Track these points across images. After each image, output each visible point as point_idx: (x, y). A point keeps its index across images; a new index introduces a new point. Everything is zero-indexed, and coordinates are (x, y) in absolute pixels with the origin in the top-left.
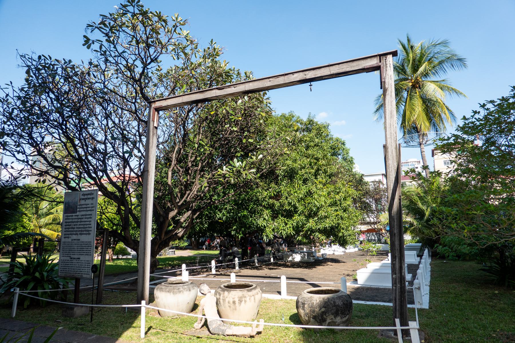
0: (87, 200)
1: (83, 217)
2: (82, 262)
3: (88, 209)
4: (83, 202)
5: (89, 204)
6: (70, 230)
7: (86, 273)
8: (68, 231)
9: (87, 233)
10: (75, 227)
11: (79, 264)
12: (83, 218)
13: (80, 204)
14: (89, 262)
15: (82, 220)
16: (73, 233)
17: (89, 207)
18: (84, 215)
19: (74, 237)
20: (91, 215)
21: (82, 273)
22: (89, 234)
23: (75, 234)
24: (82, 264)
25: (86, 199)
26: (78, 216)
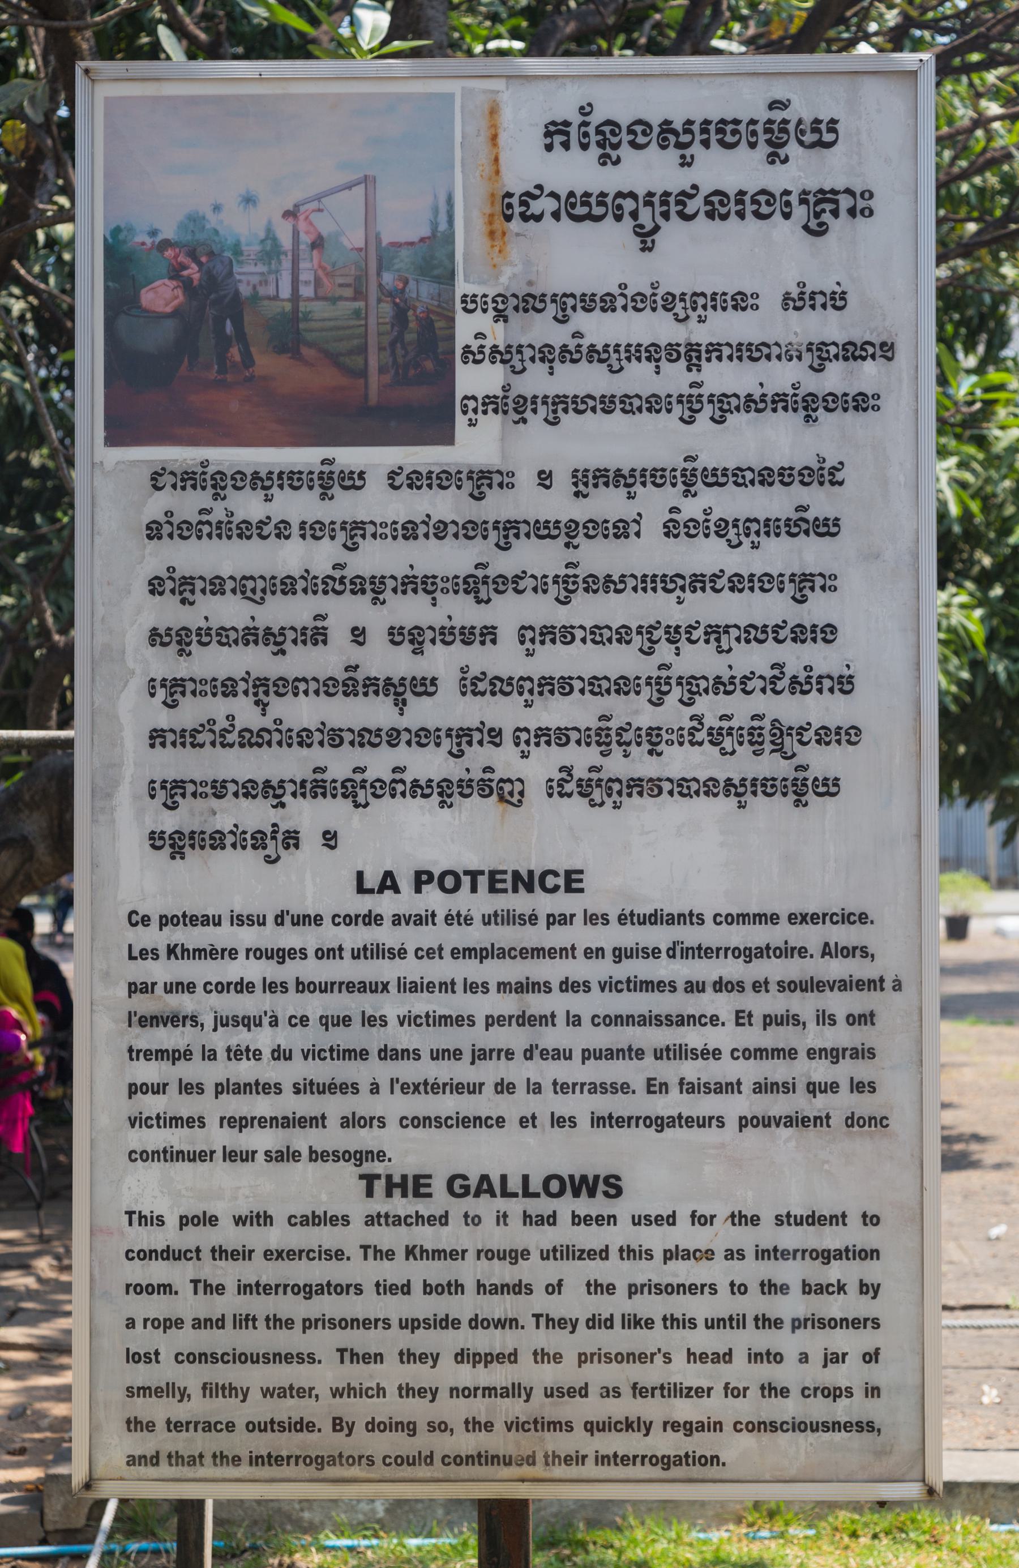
5: (741, 302)
7: (789, 1408)
12: (621, 530)
14: (854, 1235)
21: (684, 1410)
24: (682, 1272)
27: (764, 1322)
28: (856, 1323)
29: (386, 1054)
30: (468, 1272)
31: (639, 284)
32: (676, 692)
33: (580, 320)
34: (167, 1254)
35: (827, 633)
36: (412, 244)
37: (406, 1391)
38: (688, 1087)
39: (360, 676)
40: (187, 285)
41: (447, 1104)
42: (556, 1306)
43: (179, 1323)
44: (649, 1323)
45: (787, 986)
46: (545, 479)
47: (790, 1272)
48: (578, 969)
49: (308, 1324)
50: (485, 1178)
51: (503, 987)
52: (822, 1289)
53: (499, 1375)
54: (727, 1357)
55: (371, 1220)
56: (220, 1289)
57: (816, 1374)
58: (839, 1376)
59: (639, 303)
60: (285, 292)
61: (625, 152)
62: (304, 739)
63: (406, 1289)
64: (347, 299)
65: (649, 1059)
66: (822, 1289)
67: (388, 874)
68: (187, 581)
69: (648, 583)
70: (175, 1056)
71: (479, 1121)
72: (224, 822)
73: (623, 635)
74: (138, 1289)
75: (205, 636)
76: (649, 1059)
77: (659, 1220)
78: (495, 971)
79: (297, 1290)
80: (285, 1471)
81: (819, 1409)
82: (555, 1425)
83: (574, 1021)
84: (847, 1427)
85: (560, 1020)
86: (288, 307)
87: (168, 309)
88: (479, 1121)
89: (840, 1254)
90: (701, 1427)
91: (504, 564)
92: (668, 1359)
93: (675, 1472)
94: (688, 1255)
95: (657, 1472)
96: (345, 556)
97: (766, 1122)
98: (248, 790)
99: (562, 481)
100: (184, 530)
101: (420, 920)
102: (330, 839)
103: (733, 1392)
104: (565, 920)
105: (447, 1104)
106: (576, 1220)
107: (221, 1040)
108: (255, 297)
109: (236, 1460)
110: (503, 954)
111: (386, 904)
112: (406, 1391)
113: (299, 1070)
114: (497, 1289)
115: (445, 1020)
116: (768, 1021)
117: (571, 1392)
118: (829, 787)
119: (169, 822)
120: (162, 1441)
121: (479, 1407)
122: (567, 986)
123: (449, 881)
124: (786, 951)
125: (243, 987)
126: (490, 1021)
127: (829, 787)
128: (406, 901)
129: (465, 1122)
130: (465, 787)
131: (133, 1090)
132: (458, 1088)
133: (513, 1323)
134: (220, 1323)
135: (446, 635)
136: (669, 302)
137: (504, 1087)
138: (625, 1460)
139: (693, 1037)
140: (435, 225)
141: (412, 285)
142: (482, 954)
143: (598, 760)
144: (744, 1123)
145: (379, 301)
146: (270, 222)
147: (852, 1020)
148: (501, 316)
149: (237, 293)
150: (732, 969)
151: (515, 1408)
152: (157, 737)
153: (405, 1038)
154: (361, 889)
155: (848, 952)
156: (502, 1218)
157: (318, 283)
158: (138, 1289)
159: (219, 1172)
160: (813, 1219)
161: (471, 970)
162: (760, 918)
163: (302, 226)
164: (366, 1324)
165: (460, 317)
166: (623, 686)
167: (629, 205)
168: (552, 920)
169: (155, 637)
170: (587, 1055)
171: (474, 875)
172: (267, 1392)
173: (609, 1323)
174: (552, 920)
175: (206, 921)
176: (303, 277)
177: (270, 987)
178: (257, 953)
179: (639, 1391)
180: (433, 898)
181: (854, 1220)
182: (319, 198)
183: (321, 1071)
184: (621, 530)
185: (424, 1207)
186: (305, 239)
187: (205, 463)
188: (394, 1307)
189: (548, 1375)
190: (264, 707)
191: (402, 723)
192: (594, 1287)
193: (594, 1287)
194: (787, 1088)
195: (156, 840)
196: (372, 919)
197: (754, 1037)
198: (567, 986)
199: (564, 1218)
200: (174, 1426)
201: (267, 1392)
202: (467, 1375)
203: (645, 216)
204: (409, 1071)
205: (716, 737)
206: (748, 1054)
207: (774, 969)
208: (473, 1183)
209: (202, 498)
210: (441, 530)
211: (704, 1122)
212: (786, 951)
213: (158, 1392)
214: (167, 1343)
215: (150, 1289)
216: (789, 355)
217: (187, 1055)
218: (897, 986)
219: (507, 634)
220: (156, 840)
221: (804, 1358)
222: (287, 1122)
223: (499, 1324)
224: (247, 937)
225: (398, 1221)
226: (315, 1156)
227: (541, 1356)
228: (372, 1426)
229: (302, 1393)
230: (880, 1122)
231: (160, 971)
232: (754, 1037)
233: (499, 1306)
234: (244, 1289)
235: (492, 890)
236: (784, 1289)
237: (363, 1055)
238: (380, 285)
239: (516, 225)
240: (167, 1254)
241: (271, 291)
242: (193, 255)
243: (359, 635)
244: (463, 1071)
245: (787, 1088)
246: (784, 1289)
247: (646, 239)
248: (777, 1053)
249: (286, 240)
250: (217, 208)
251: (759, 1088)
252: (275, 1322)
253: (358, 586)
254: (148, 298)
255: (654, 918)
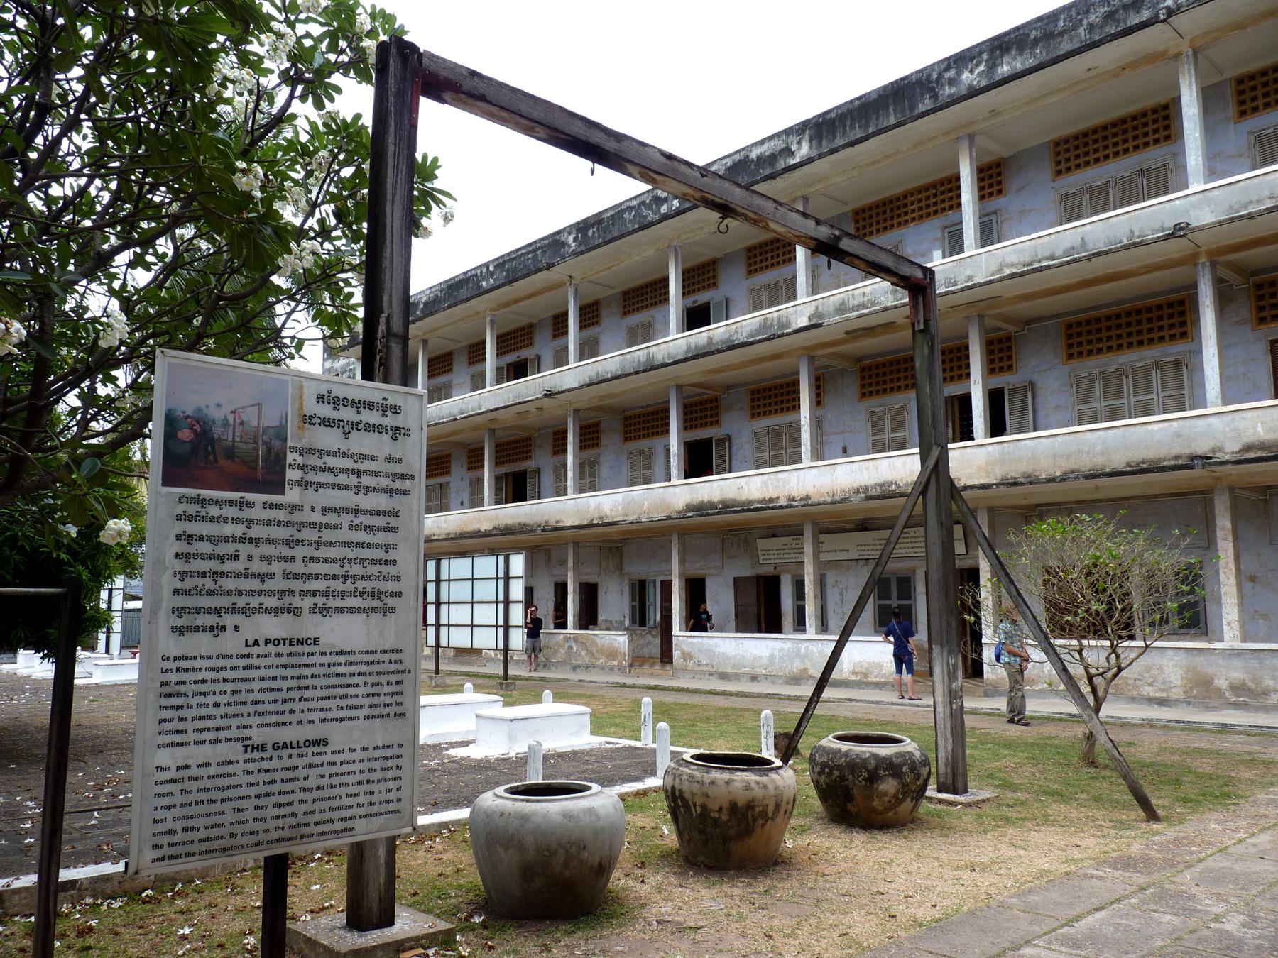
0: (354, 433)
1: (332, 518)
2: (347, 756)
3: (367, 481)
4: (329, 439)
5: (373, 458)
6: (229, 584)
7: (375, 809)
8: (211, 593)
9: (376, 603)
10: (276, 567)
11: (326, 770)
12: (336, 527)
13: (304, 443)
14: (395, 751)
15: (327, 535)
16: (254, 602)
17: (375, 474)
18: (347, 511)
19: (271, 627)
20: (394, 514)
21: (345, 814)
22: (385, 611)
23: (277, 612)
24: (346, 768)
25: (355, 425)
26: (293, 508)
27: (370, 782)
28: (395, 779)
29: (254, 702)
30: (278, 776)
31: (344, 449)
32: (350, 580)
33: (326, 458)
34: (171, 781)
35: (394, 562)
37: (256, 820)
38: (349, 708)
39: (250, 571)
40: (195, 432)
41: (274, 719)
42: (307, 784)
43: (175, 806)
44: (335, 786)
45: (379, 673)
46: (313, 509)
47: (377, 765)
48: (317, 670)
49: (223, 801)
50: (285, 743)
51: (293, 677)
52: (386, 769)
53: (287, 810)
54: (358, 795)
55: (246, 761)
56: (191, 792)
57: (384, 797)
58: (391, 796)
59: (344, 455)
60: (230, 438)
61: (341, 406)
62: (229, 593)
63: (257, 784)
65: (338, 699)
66: (386, 769)
67: (256, 640)
68: (190, 536)
69: (343, 544)
70: (177, 708)
71: (284, 724)
72: (199, 622)
73: (335, 561)
74: (159, 795)
75: (197, 556)
76: (338, 699)
77: (339, 752)
78: (290, 672)
79: (219, 789)
80: (212, 855)
81: (384, 808)
82: (305, 825)
83: (315, 688)
84: (392, 812)
85: (311, 687)
88: (284, 724)
89: (392, 757)
90: (350, 818)
91: (299, 536)
92: (340, 797)
93: (341, 835)
94: (348, 762)
95: (336, 836)
96: (247, 530)
97: (372, 717)
98: (209, 611)
99: (318, 508)
100: (190, 518)
101: (266, 656)
102: (237, 628)
103: (359, 806)
104: (313, 654)
105: (274, 719)
106: (314, 754)
107: (194, 701)
108: (219, 439)
109: (194, 854)
110: (293, 666)
111: (255, 650)
112: (256, 820)
113: (223, 710)
114: (287, 781)
115: (274, 690)
116: (373, 685)
117: (310, 813)
118: (393, 610)
119: (179, 623)
120: (166, 851)
121: (280, 822)
122: (313, 676)
123: (276, 642)
124: (379, 662)
125: (204, 681)
126: (288, 689)
127: (393, 610)
128: (261, 649)
129: (279, 724)
130: (283, 610)
131: (160, 721)
132: (277, 713)
133: (292, 792)
134: (191, 804)
135: (279, 559)
136: (353, 456)
137: (292, 712)
138: (326, 833)
139: (351, 691)
140: (281, 422)
142: (286, 667)
143: (325, 601)
144: (365, 718)
147: (397, 683)
148: (301, 454)
150: (363, 668)
151: (292, 821)
152: (176, 592)
153: (259, 697)
154: (247, 645)
155: (396, 662)
156: (290, 756)
157: (241, 436)
158: (159, 795)
159: (192, 749)
160: (384, 747)
161: (283, 672)
162: (372, 652)
164: (243, 798)
165: (288, 453)
166: (334, 577)
167: (342, 424)
168: (309, 655)
169: (177, 556)
170: (319, 699)
171: (284, 640)
172: (207, 827)
173: (323, 788)
174: (309, 655)
175: (191, 658)
176: (237, 434)
177: (214, 681)
178: (210, 669)
179: (332, 809)
180: (271, 648)
181: (395, 746)
182: (243, 408)
183: (230, 710)
184: (336, 527)
185: (265, 755)
186: (238, 421)
187: (199, 495)
188: (253, 791)
189: (304, 808)
190: (215, 581)
191: (263, 588)
192: (319, 776)
193: (319, 776)
194: (378, 706)
195: (174, 629)
196: (250, 656)
197: (369, 690)
198: (313, 676)
199: (310, 754)
200: (171, 845)
201: (207, 827)
202: (277, 812)
203: (346, 428)
204: (260, 708)
205: (361, 594)
206: (367, 696)
207: (375, 668)
208: (281, 745)
209: (197, 507)
210: (279, 523)
211: (353, 719)
212: (379, 662)
213: (166, 833)
214: (169, 815)
215: (164, 795)
216: (387, 476)
217: (182, 707)
218: (410, 672)
219: (299, 559)
220: (174, 629)
221: (380, 792)
222: (217, 729)
223: (288, 792)
224: (207, 663)
225: (256, 760)
226: (227, 740)
227: (301, 802)
228: (243, 834)
229: (219, 826)
230: (403, 715)
231: (173, 677)
232: (369, 690)
233: (288, 786)
234: (200, 791)
235: (290, 645)
236: (375, 770)
237: (245, 703)
239: (307, 425)
240: (171, 781)
242: (198, 423)
243: (250, 558)
244: (279, 707)
245: (378, 706)
246: (375, 770)
247: (346, 434)
248: (375, 695)
249: (231, 422)
250: (207, 407)
251: (370, 706)
252: (211, 801)
253: (251, 541)
254: (180, 435)
255: (341, 653)
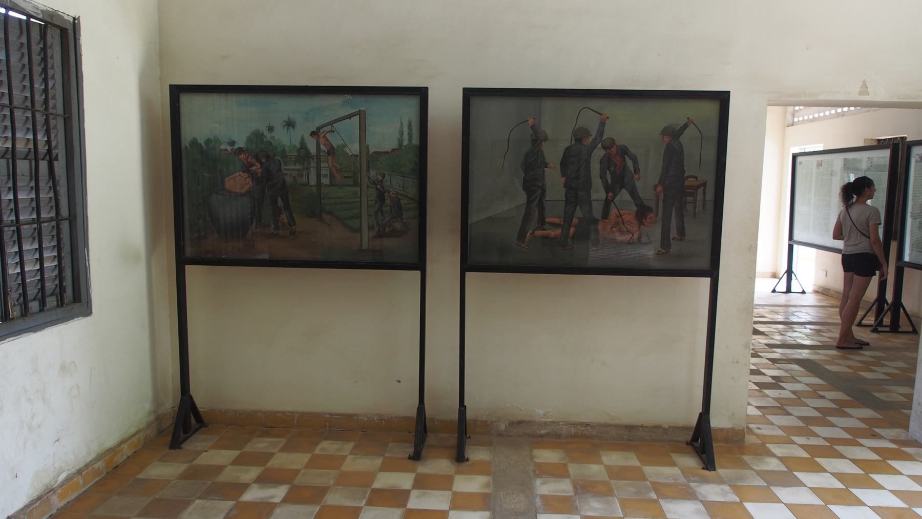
36: (387, 153)
60: (313, 181)
64: (349, 186)
86: (314, 190)
87: (243, 191)
141: (387, 178)
145: (368, 187)
146: (303, 138)
149: (284, 182)
157: (332, 176)
163: (322, 140)
182: (331, 123)
238: (369, 177)
241: (304, 180)
242: (257, 157)
249: (313, 149)
250: (271, 129)
254: (229, 184)
